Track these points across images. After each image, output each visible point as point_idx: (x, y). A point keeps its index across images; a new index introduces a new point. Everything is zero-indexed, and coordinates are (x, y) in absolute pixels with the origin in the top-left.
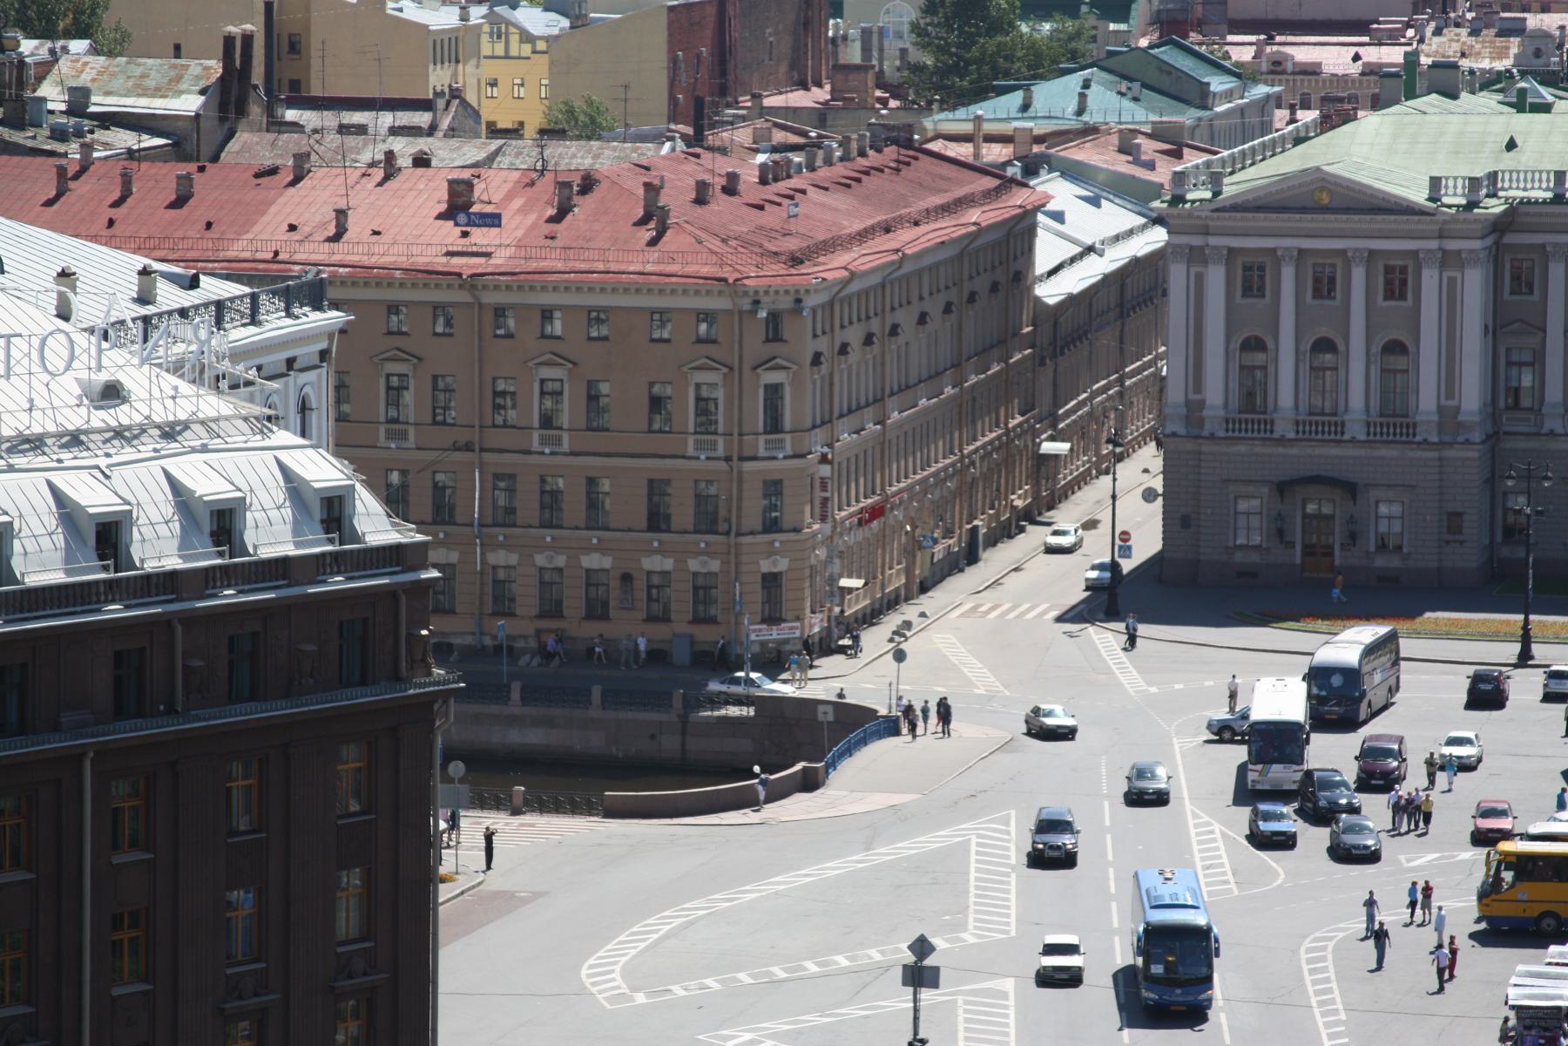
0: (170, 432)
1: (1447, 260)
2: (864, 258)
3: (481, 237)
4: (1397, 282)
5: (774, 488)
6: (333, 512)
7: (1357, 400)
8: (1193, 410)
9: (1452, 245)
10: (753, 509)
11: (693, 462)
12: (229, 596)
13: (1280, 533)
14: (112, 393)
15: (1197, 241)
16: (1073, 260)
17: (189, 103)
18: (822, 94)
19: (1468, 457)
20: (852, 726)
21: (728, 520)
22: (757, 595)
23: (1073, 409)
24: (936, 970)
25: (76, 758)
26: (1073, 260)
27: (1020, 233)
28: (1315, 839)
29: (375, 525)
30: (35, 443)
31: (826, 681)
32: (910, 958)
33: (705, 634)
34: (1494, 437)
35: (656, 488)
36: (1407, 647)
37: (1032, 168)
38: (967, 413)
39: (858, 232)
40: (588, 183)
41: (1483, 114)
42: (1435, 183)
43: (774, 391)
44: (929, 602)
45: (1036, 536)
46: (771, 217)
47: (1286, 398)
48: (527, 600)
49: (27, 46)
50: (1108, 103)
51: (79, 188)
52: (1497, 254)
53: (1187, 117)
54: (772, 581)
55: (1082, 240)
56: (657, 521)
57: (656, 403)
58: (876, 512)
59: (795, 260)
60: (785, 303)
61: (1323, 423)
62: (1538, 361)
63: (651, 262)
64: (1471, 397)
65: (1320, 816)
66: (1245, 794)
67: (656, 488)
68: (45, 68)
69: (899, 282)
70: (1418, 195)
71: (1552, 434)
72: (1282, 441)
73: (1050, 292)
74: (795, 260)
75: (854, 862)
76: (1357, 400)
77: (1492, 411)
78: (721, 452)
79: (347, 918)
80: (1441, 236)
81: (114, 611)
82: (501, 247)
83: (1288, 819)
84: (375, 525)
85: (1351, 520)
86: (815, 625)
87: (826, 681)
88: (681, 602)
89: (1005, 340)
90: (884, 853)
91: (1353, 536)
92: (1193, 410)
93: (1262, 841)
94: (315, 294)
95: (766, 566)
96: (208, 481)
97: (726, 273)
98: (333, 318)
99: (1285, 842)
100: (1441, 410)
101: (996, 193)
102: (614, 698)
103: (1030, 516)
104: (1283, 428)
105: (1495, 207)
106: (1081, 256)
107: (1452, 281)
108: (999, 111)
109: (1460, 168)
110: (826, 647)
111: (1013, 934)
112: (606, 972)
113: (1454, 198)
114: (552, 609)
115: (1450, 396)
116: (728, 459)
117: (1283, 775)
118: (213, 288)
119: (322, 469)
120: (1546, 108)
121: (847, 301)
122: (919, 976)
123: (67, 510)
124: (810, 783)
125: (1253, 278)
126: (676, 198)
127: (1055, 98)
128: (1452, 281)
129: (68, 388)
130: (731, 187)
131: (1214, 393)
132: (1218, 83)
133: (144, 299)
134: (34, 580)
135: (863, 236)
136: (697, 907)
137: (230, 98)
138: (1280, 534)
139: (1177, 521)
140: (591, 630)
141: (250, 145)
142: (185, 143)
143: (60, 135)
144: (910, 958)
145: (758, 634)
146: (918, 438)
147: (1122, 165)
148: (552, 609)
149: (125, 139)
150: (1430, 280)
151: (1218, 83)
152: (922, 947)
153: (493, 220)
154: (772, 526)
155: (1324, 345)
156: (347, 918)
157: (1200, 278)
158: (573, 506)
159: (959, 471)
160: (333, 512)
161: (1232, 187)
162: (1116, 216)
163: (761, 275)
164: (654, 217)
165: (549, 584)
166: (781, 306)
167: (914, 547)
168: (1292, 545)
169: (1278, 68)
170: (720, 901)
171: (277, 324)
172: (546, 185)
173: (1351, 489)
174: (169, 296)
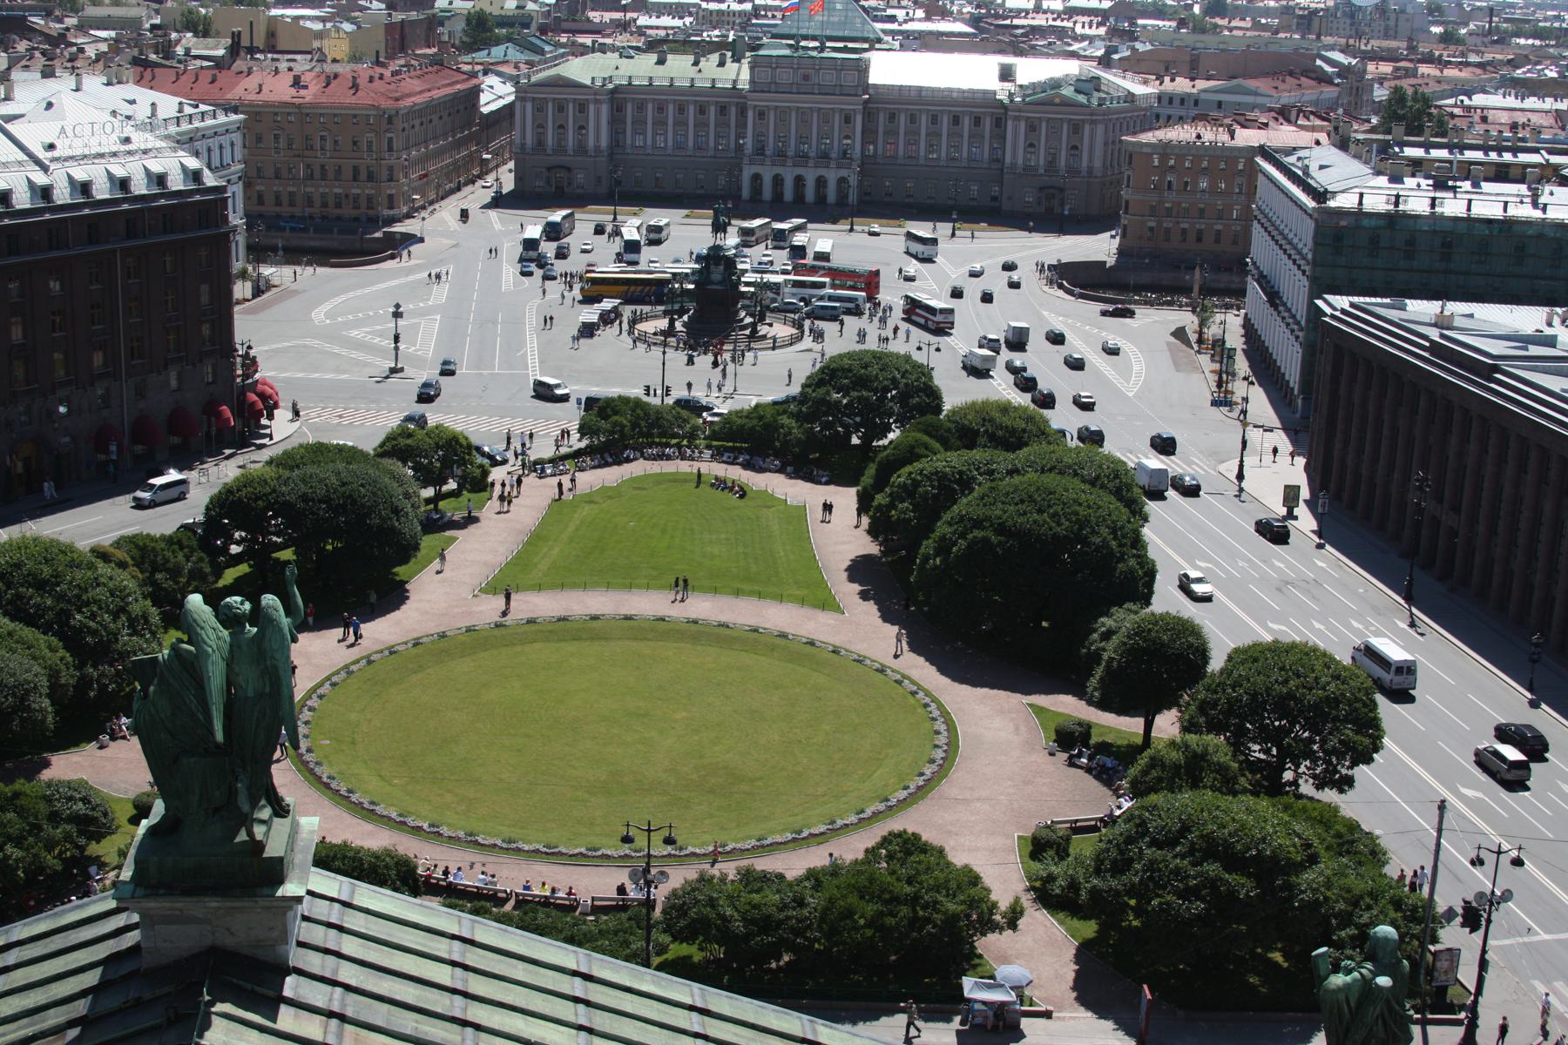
0: (145, 152)
1: (597, 102)
2: (418, 99)
3: (303, 92)
4: (582, 107)
5: (391, 168)
7: (571, 143)
8: (523, 145)
10: (385, 174)
12: (163, 202)
14: (127, 140)
17: (221, 52)
18: (435, 50)
22: (386, 201)
23: (493, 145)
25: (115, 251)
27: (476, 91)
28: (539, 273)
30: (102, 156)
31: (398, 228)
33: (371, 212)
34: (611, 155)
36: (577, 216)
37: (486, 73)
38: (458, 145)
39: (418, 89)
40: (336, 76)
41: (612, 58)
43: (390, 140)
44: (443, 203)
45: (480, 183)
46: (393, 86)
47: (550, 142)
48: (318, 203)
49: (174, 35)
50: (514, 54)
51: (183, 78)
52: (612, 100)
53: (536, 58)
54: (391, 197)
55: (495, 94)
57: (355, 143)
58: (425, 176)
59: (397, 100)
61: (560, 149)
62: (624, 132)
63: (353, 100)
64: (604, 143)
65: (541, 266)
66: (521, 260)
67: (356, 170)
68: (178, 41)
69: (432, 107)
70: (588, 82)
73: (485, 110)
74: (397, 100)
75: (402, 280)
76: (571, 143)
79: (205, 299)
81: (126, 206)
82: (308, 96)
83: (533, 267)
84: (210, 180)
86: (405, 210)
87: (398, 228)
88: (363, 202)
89: (470, 124)
90: (411, 278)
92: (523, 145)
93: (523, 274)
94: (236, 110)
96: (156, 167)
98: (241, 116)
99: (530, 274)
102: (340, 232)
103: (480, 177)
104: (549, 151)
105: (611, 86)
108: (481, 56)
109: (600, 75)
110: (409, 216)
112: (319, 314)
113: (599, 83)
114: (325, 205)
117: (532, 254)
118: (203, 108)
119: (193, 163)
121: (414, 112)
122: (397, 315)
123: (110, 176)
124: (392, 257)
125: (540, 108)
126: (363, 82)
127: (498, 52)
129: (114, 137)
130: (381, 77)
131: (529, 141)
132: (547, 48)
133: (180, 111)
134: (99, 197)
135: (421, 92)
136: (351, 294)
137: (235, 50)
138: (548, 182)
139: (518, 179)
140: (337, 211)
141: (240, 64)
142: (219, 64)
143: (180, 62)
145: (386, 212)
146: (439, 153)
148: (325, 205)
149: (198, 63)
150: (592, 107)
151: (547, 48)
152: (398, 306)
153: (306, 87)
154: (391, 180)
155: (561, 127)
156: (205, 299)
158: (331, 175)
159: (455, 163)
160: (196, 176)
161: (534, 79)
163: (385, 104)
164: (355, 86)
167: (439, 186)
169: (574, 43)
170: (359, 292)
171: (222, 118)
172: (323, 77)
173: (569, 170)
174: (188, 110)
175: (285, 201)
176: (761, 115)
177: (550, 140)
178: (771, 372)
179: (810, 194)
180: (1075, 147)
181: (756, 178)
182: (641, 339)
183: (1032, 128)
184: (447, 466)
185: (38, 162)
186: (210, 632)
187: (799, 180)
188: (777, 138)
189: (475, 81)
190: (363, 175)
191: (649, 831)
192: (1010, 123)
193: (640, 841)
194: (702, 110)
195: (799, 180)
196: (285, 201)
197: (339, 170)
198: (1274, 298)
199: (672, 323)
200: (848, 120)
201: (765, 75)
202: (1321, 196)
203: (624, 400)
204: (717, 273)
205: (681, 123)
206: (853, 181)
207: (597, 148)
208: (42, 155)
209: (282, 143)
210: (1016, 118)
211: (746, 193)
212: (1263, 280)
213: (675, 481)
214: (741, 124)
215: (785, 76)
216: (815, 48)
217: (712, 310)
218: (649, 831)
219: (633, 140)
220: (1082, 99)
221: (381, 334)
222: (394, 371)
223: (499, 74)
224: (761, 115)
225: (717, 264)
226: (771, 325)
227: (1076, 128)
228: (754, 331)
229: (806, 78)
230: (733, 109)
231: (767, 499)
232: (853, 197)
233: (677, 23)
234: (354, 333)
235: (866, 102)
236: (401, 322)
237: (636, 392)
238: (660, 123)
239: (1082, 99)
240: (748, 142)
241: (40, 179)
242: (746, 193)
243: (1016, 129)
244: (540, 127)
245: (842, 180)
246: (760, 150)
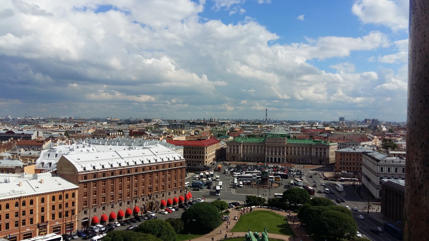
4: (238, 147)
6: (180, 158)
25: (166, 170)
29: (182, 158)
119: (180, 156)
180: (325, 152)
181: (268, 158)
183: (317, 149)
185: (154, 154)
192: (313, 149)
198: (369, 180)
200: (283, 148)
202: (378, 161)
206: (285, 159)
208: (155, 154)
210: (314, 148)
211: (266, 160)
212: (366, 177)
220: (325, 144)
224: (268, 147)
227: (325, 149)
233: (251, 132)
239: (325, 144)
241: (156, 158)
242: (266, 160)
243: (314, 150)
244: (230, 150)
245: (283, 159)
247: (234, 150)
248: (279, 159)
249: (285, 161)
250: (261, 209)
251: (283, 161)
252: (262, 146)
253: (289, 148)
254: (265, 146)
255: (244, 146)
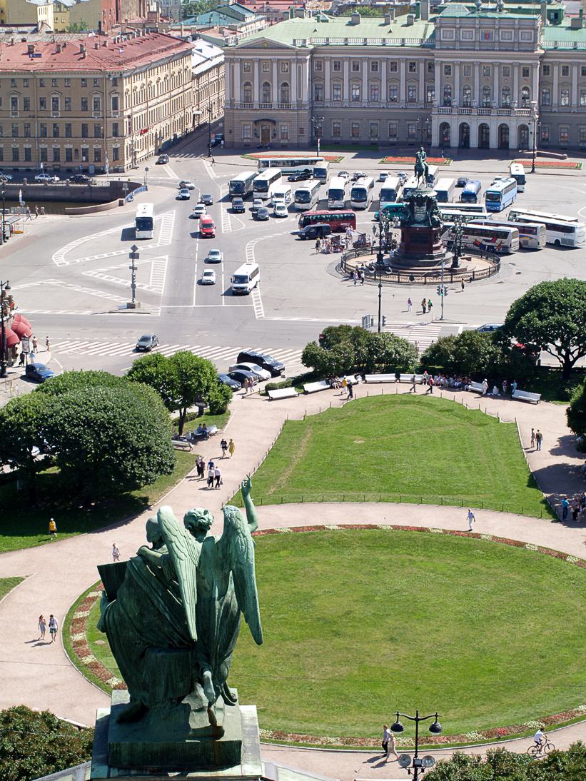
1: (298, 61)
3: (36, 60)
9: (299, 57)
10: (110, 131)
11: (92, 119)
13: (256, 134)
15: (232, 57)
16: (203, 62)
19: (305, 113)
20: (134, 186)
21: (103, 134)
24: (138, 254)
26: (203, 62)
32: (132, 251)
34: (312, 108)
35: (85, 127)
37: (194, 39)
42: (294, 41)
46: (115, 53)
47: (256, 99)
52: (312, 59)
54: (116, 150)
56: (85, 135)
60: (118, 76)
62: (323, 87)
64: (306, 98)
67: (85, 127)
70: (289, 43)
71: (327, 107)
72: (256, 110)
73: (197, 71)
74: (120, 64)
77: (312, 102)
78: (101, 116)
80: (297, 55)
82: (39, 64)
85: (274, 130)
91: (275, 135)
92: (231, 103)
95: (114, 146)
97: (102, 68)
100: (297, 101)
101: (180, 44)
106: (205, 61)
107: (300, 67)
111: (170, 242)
113: (299, 44)
114: (57, 158)
115: (300, 97)
116: (103, 118)
120: (327, 21)
128: (300, 67)
132: (247, 15)
144: (132, 251)
147: (219, 37)
150: (294, 66)
153: (39, 56)
157: (233, 66)
158: (62, 132)
162: (217, 50)
165: (56, 151)
166: (116, 76)
168: (259, 137)
172: (54, 47)
173: (274, 122)
175: (22, 155)
176: (448, 70)
177: (256, 95)
178: (478, 302)
179: (494, 141)
181: (445, 126)
182: (351, 275)
184: (190, 390)
186: (182, 539)
187: (484, 129)
188: (463, 90)
189: (187, 46)
190: (91, 132)
191: (417, 720)
193: (410, 728)
194: (394, 66)
195: (484, 129)
196: (22, 155)
197: (68, 127)
199: (380, 257)
200: (526, 73)
201: (447, 35)
203: (345, 329)
204: (421, 213)
205: (374, 79)
206: (533, 128)
207: (300, 105)
209: (20, 104)
211: (435, 140)
213: (393, 402)
214: (430, 78)
215: (468, 35)
216: (493, 10)
217: (416, 243)
218: (417, 720)
219: (559, 101)
221: (116, 273)
222: (131, 306)
223: (206, 39)
224: (448, 70)
225: (420, 205)
226: (469, 259)
228: (455, 264)
229: (487, 36)
230: (422, 66)
231: (481, 420)
232: (533, 141)
234: (93, 273)
235: (542, 57)
236: (137, 263)
237: (355, 322)
238: (356, 79)
240: (437, 96)
242: (435, 140)
245: (523, 128)
246: (447, 103)
247: (266, 85)
248: (503, 130)
249: (533, 141)
250: (389, 390)
251: (523, 144)
252: (412, 66)
253: (556, 73)
254: (431, 67)
255: (317, 64)
